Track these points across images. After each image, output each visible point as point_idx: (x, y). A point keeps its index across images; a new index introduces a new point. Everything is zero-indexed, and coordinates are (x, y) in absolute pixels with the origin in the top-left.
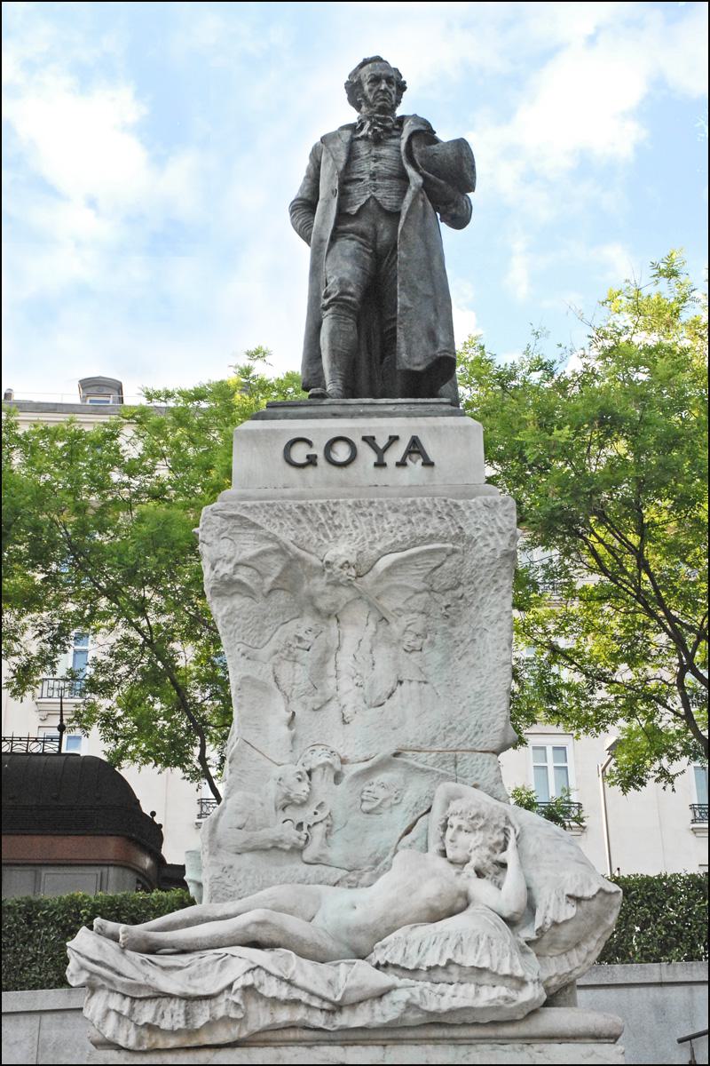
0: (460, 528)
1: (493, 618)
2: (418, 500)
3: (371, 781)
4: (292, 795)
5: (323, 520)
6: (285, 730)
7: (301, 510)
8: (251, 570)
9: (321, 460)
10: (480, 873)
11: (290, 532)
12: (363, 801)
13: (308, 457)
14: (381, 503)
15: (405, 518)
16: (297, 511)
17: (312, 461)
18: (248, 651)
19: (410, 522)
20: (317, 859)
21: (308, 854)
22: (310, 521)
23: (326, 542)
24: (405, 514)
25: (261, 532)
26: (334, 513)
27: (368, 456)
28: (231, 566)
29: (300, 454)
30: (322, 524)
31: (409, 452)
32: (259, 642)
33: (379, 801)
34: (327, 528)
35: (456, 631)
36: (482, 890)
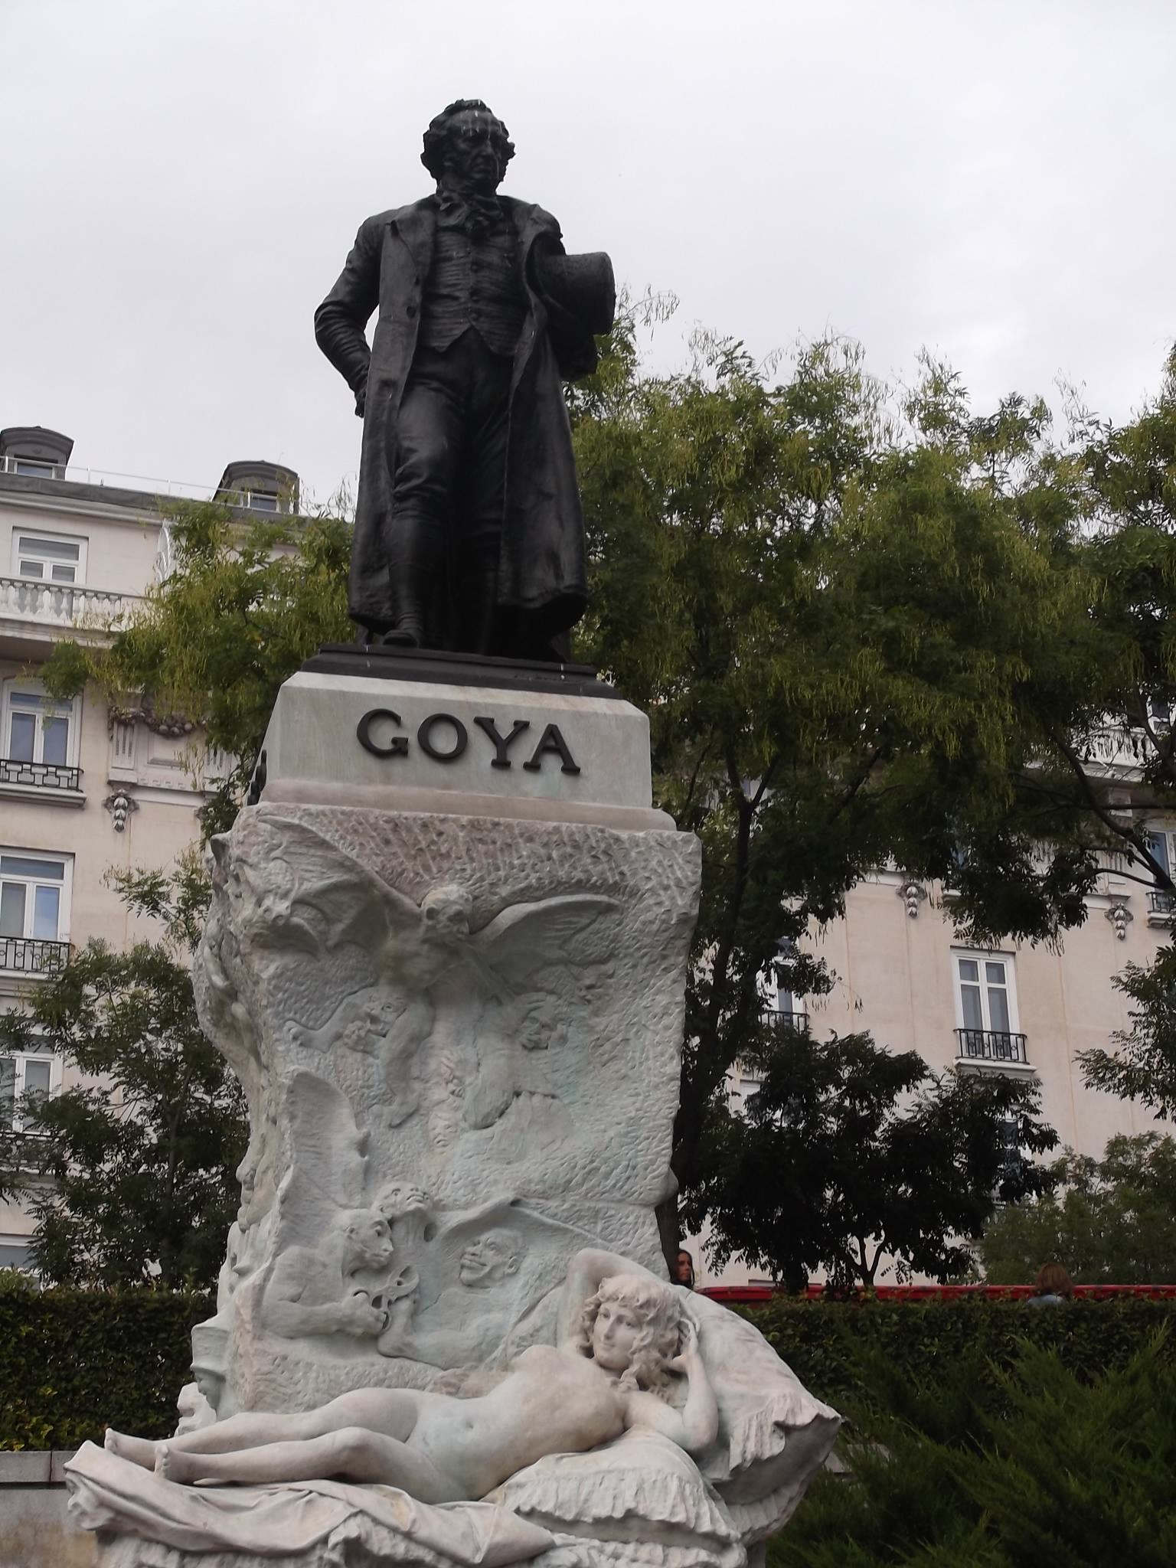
0: (622, 873)
1: (658, 1010)
2: (564, 826)
3: (476, 1239)
5: (423, 845)
6: (355, 1159)
7: (391, 825)
8: (314, 912)
10: (643, 1385)
11: (374, 858)
12: (463, 1267)
13: (395, 741)
14: (509, 827)
15: (542, 852)
16: (386, 826)
17: (400, 749)
18: (301, 1034)
19: (550, 858)
20: (400, 1350)
21: (387, 1343)
22: (404, 844)
23: (427, 878)
24: (545, 845)
25: (332, 855)
26: (440, 834)
27: (483, 750)
28: (287, 903)
30: (421, 850)
31: (544, 749)
32: (317, 1020)
33: (487, 1269)
34: (428, 856)
35: (600, 1022)
36: (646, 1406)
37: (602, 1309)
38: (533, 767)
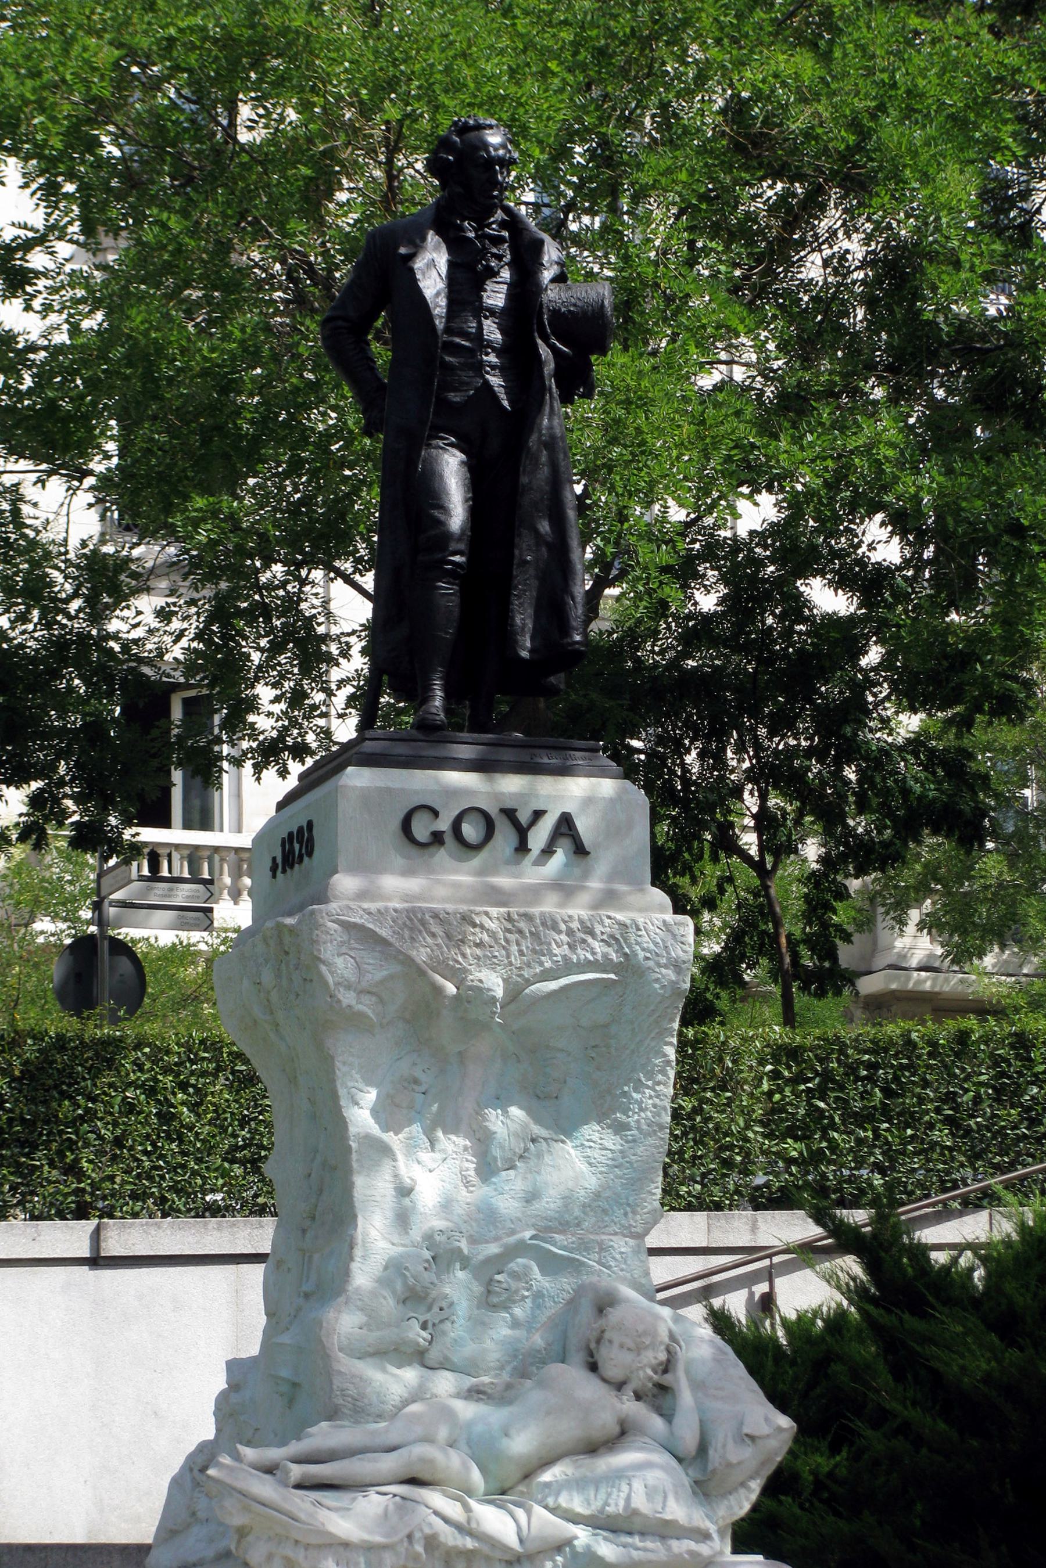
4: (418, 1288)
8: (374, 999)
9: (449, 838)
17: (437, 838)
37: (607, 1335)
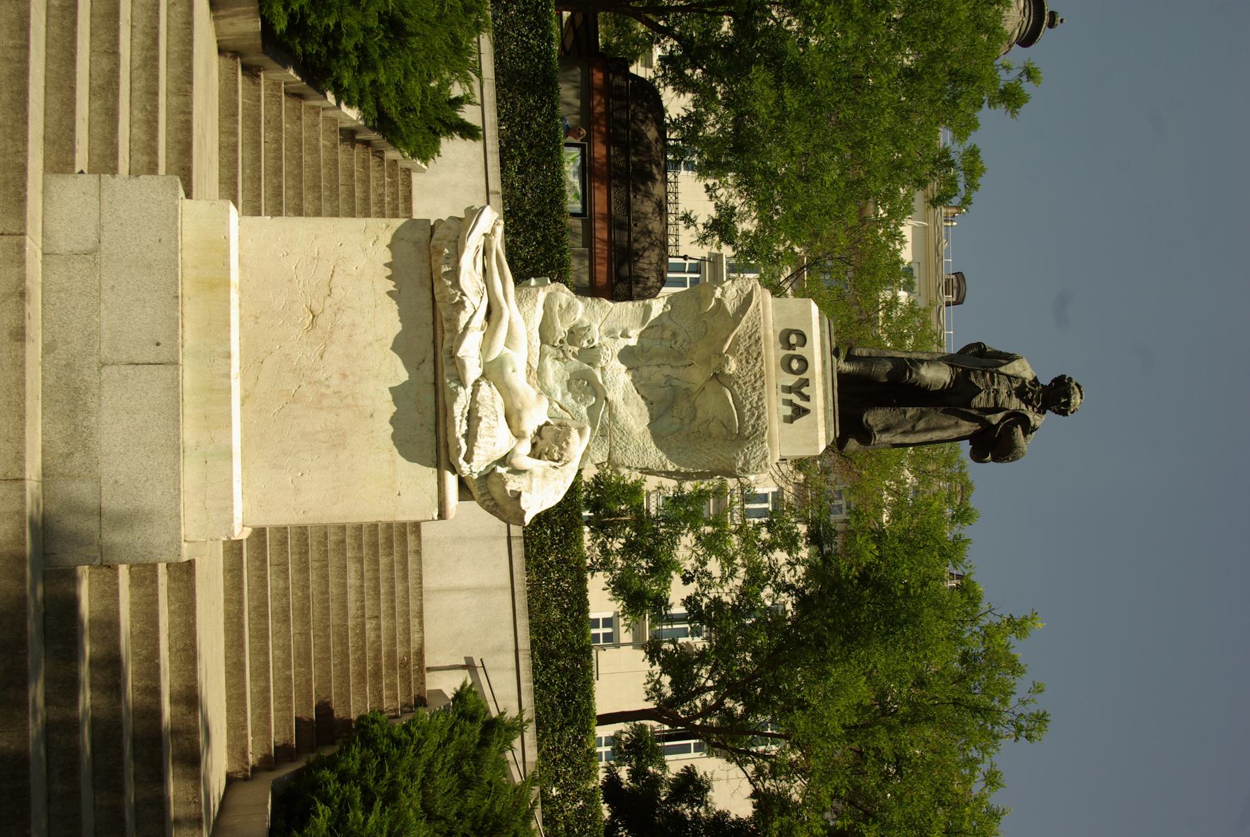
21: (547, 348)
29: (793, 339)
36: (526, 446)
38: (790, 403)
